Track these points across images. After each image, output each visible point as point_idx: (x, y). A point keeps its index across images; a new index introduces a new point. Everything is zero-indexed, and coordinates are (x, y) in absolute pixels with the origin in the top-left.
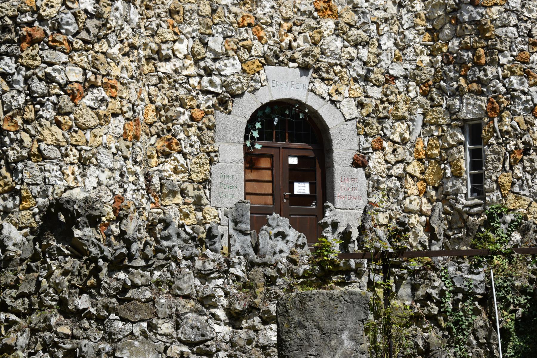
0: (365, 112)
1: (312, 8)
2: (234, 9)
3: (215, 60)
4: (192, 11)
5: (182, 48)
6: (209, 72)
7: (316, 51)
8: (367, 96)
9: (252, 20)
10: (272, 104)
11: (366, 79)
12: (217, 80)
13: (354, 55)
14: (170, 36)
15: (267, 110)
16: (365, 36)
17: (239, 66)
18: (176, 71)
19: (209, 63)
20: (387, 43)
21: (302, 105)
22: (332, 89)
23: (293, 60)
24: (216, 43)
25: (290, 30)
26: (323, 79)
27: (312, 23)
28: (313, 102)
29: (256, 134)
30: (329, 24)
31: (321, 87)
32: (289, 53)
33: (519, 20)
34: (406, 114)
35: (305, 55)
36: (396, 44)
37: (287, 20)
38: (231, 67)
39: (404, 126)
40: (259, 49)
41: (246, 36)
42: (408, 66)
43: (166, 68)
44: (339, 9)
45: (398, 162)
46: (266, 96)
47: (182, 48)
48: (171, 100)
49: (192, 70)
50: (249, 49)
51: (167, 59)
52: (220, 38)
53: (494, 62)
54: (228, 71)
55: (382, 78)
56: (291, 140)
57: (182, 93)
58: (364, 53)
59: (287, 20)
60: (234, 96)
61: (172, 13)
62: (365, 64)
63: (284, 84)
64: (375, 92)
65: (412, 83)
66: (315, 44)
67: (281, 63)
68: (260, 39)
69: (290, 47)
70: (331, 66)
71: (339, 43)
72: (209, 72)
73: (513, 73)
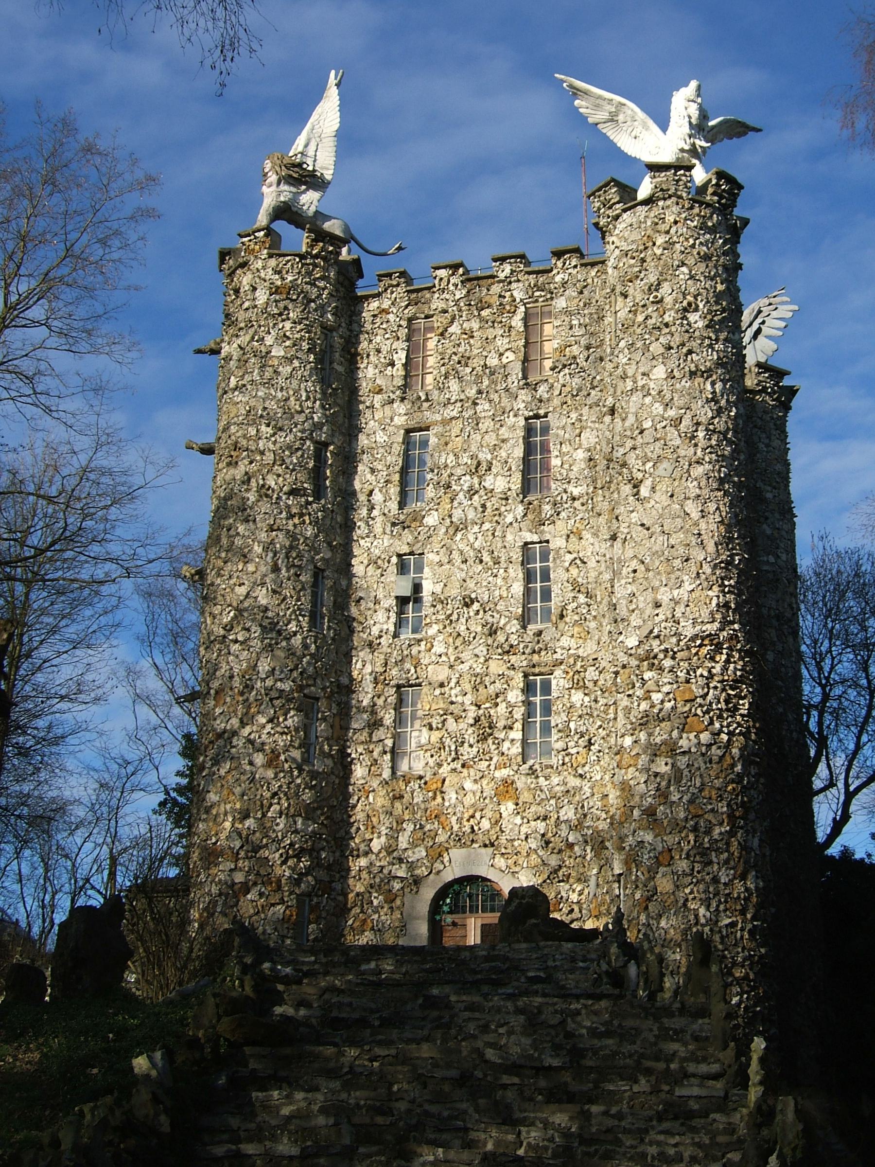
28: (491, 875)
29: (446, 909)
30: (508, 807)
31: (500, 862)
32: (471, 836)
46: (449, 876)
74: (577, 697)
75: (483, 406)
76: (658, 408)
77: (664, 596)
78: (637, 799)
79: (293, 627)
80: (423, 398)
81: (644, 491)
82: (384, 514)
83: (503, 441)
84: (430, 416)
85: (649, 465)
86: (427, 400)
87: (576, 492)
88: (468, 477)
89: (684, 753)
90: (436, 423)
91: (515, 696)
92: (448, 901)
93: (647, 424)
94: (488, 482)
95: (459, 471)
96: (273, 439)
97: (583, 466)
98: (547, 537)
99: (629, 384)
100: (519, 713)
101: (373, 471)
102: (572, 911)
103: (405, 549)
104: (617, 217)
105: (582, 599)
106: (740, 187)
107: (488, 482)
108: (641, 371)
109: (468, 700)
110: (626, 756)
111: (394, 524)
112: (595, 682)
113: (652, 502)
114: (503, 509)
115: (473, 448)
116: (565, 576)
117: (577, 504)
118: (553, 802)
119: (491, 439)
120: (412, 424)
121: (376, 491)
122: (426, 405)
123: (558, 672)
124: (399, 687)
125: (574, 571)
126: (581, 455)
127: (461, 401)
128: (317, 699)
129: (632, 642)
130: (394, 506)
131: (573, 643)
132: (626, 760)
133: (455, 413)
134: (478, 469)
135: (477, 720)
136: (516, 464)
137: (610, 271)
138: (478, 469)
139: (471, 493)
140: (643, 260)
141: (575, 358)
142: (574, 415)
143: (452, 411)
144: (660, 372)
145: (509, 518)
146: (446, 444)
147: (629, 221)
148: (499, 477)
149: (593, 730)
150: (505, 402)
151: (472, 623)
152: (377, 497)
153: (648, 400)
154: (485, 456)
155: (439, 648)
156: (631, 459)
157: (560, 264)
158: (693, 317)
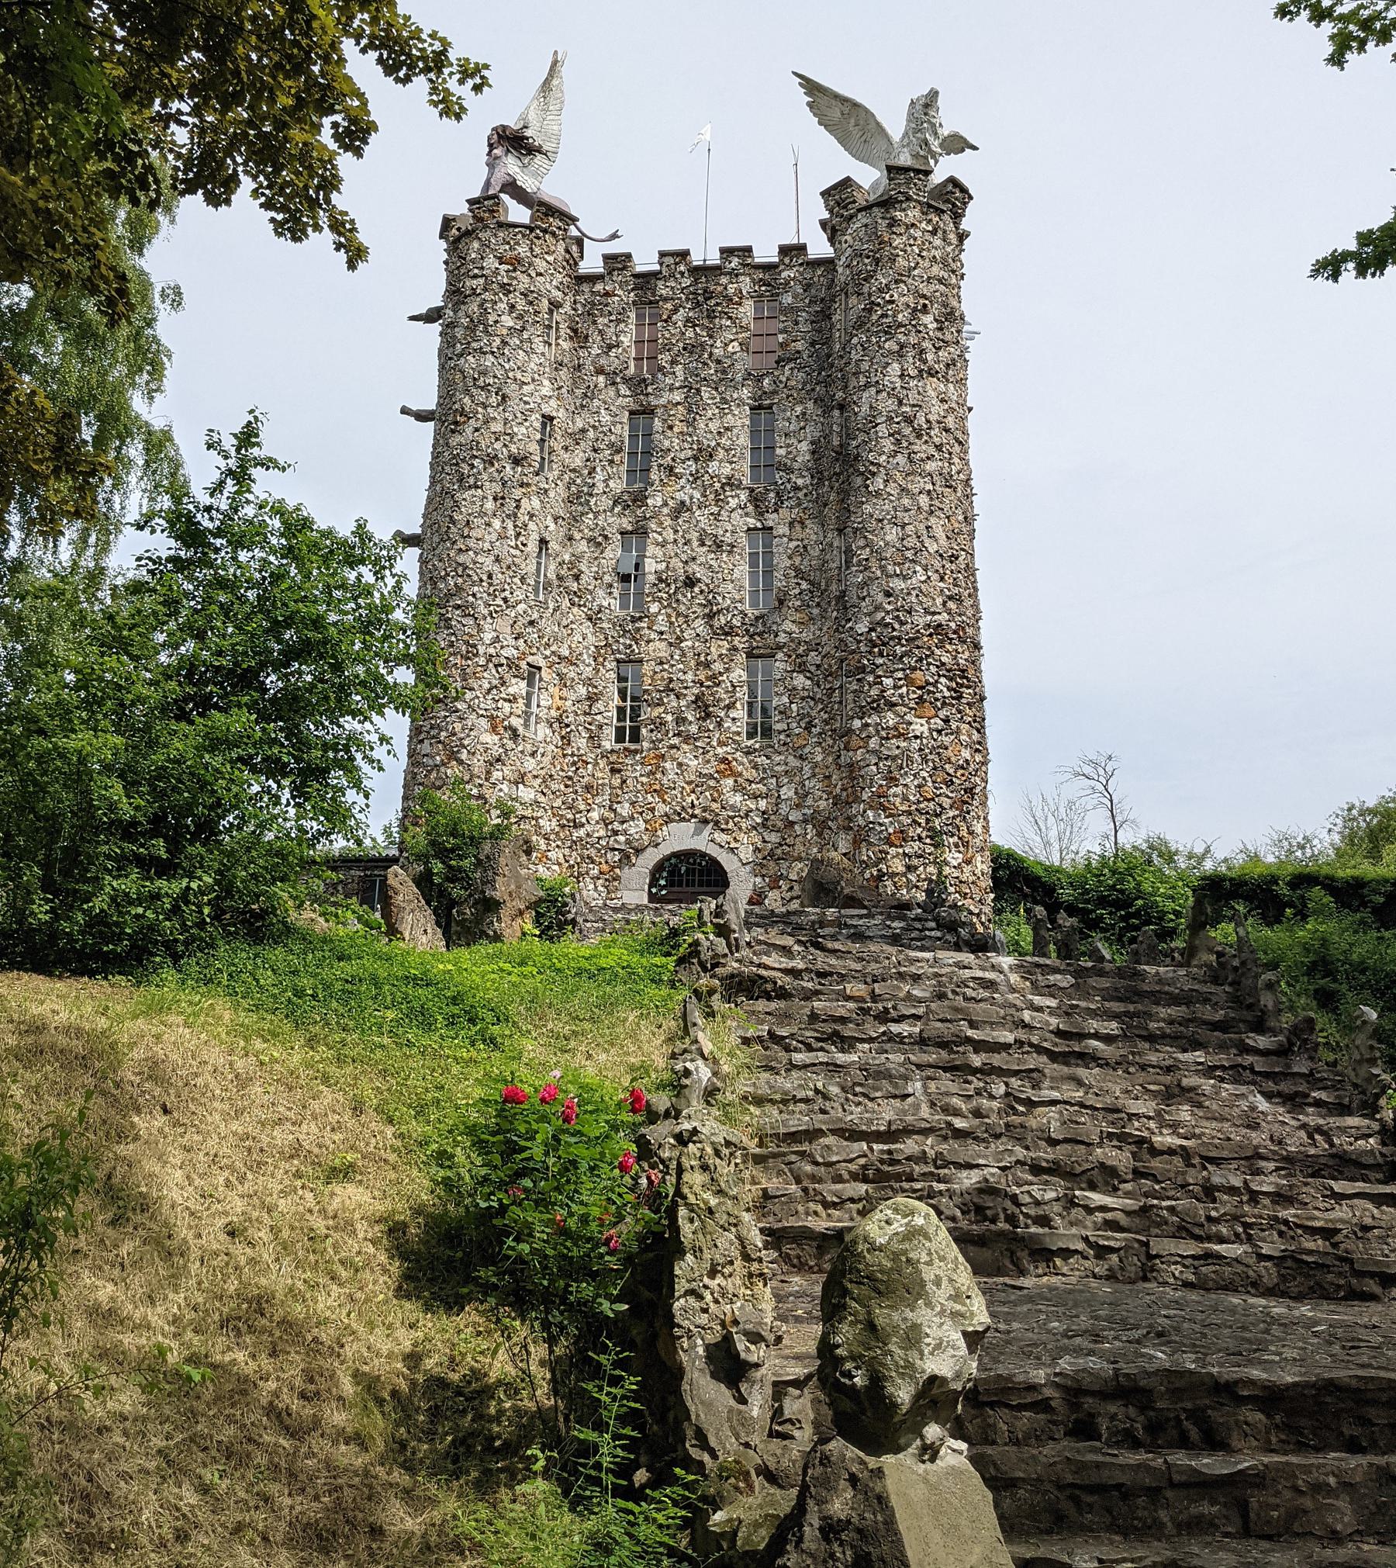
0: (760, 856)
1: (712, 771)
2: (644, 780)
3: (623, 823)
4: (603, 785)
5: (595, 815)
6: (616, 833)
7: (714, 806)
8: (764, 841)
9: (657, 787)
10: (675, 855)
11: (764, 825)
12: (622, 838)
13: (753, 807)
14: (582, 807)
15: (673, 861)
16: (764, 789)
17: (643, 825)
18: (588, 835)
19: (616, 826)
20: (788, 792)
21: (703, 855)
22: (729, 838)
23: (695, 816)
24: (624, 810)
25: (693, 792)
26: (723, 830)
27: (712, 783)
28: (713, 851)
33: (880, 759)
34: (803, 855)
35: (704, 811)
36: (796, 793)
37: (689, 783)
38: (636, 828)
39: (800, 865)
40: (662, 808)
41: (650, 799)
42: (806, 811)
43: (582, 832)
44: (740, 768)
45: (792, 898)
46: (666, 850)
47: (595, 815)
48: (582, 858)
49: (602, 833)
50: (652, 810)
51: (583, 825)
52: (627, 805)
53: (858, 800)
54: (632, 831)
55: (779, 824)
56: (701, 885)
57: (593, 852)
58: (763, 804)
59: (689, 783)
60: (638, 851)
61: (588, 788)
62: (764, 813)
63: (680, 838)
64: (774, 838)
65: (810, 826)
66: (714, 800)
67: (683, 820)
68: (664, 801)
69: (693, 806)
70: (732, 818)
71: (738, 798)
72: (616, 833)
73: (871, 808)
74: (800, 681)
76: (891, 404)
77: (897, 584)
79: (519, 595)
81: (878, 483)
83: (727, 429)
85: (884, 457)
87: (800, 482)
89: (916, 737)
91: (739, 674)
92: (665, 874)
98: (770, 523)
99: (863, 380)
100: (742, 694)
102: (791, 888)
104: (851, 217)
105: (804, 585)
106: (971, 198)
109: (690, 677)
110: (854, 737)
112: (818, 666)
116: (788, 563)
117: (801, 495)
118: (774, 781)
119: (714, 426)
120: (635, 407)
121: (598, 469)
123: (780, 655)
124: (618, 661)
125: (797, 560)
128: (539, 669)
129: (862, 628)
131: (794, 628)
132: (855, 742)
134: (703, 455)
135: (698, 698)
137: (840, 270)
138: (703, 455)
139: (696, 477)
140: (877, 261)
141: (798, 352)
142: (799, 409)
143: (677, 397)
144: (895, 367)
145: (733, 503)
147: (865, 221)
149: (813, 713)
151: (692, 602)
155: (661, 623)
157: (787, 260)
158: (927, 319)
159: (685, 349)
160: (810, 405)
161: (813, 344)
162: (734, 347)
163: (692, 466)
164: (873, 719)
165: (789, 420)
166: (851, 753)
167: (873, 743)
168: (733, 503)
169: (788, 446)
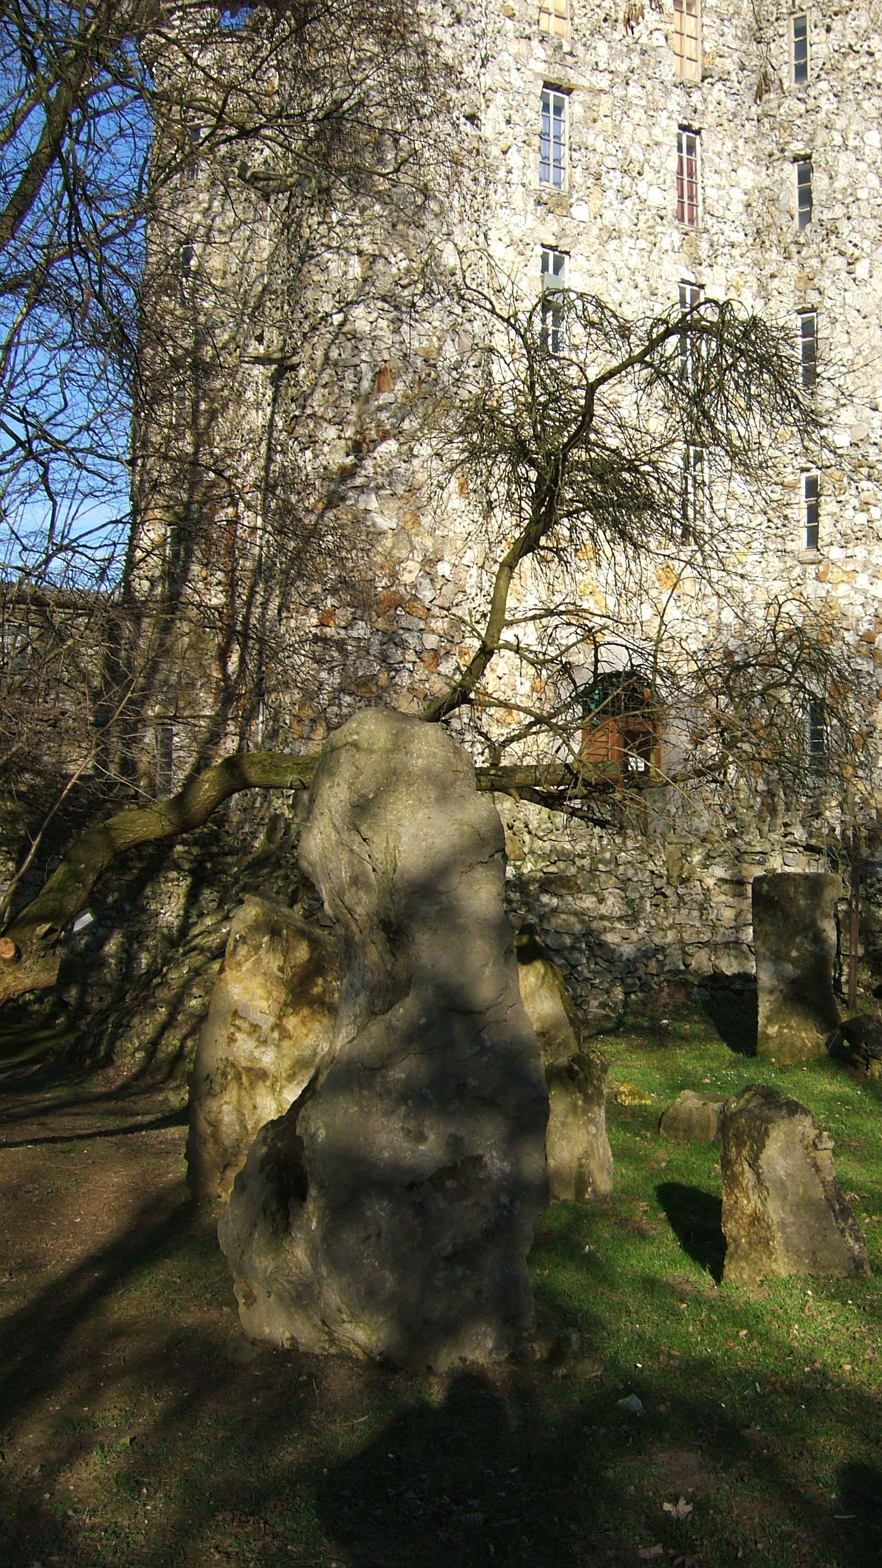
75: (634, 90)
78: (853, 621)
80: (566, 48)
81: (861, 269)
82: (524, 185)
84: (574, 77)
86: (571, 54)
88: (618, 174)
90: (582, 88)
93: (862, 194)
94: (642, 187)
95: (609, 162)
96: (450, 31)
97: (741, 208)
101: (508, 122)
103: (552, 242)
107: (642, 187)
108: (854, 127)
111: (539, 203)
113: (869, 289)
114: (659, 229)
115: (625, 140)
117: (736, 252)
119: (643, 135)
120: (552, 77)
121: (514, 149)
122: (570, 60)
126: (737, 195)
127: (611, 72)
130: (533, 177)
132: (835, 575)
133: (604, 84)
136: (671, 179)
143: (602, 81)
145: (665, 244)
146: (595, 121)
148: (654, 188)
150: (658, 94)
152: (514, 159)
153: (862, 166)
154: (636, 153)
156: (844, 227)
159: (605, 20)
160: (741, 143)
161: (743, 68)
162: (658, 39)
163: (614, 180)
164: (860, 552)
165: (719, 154)
166: (828, 586)
167: (862, 580)
168: (665, 244)
169: (720, 187)
